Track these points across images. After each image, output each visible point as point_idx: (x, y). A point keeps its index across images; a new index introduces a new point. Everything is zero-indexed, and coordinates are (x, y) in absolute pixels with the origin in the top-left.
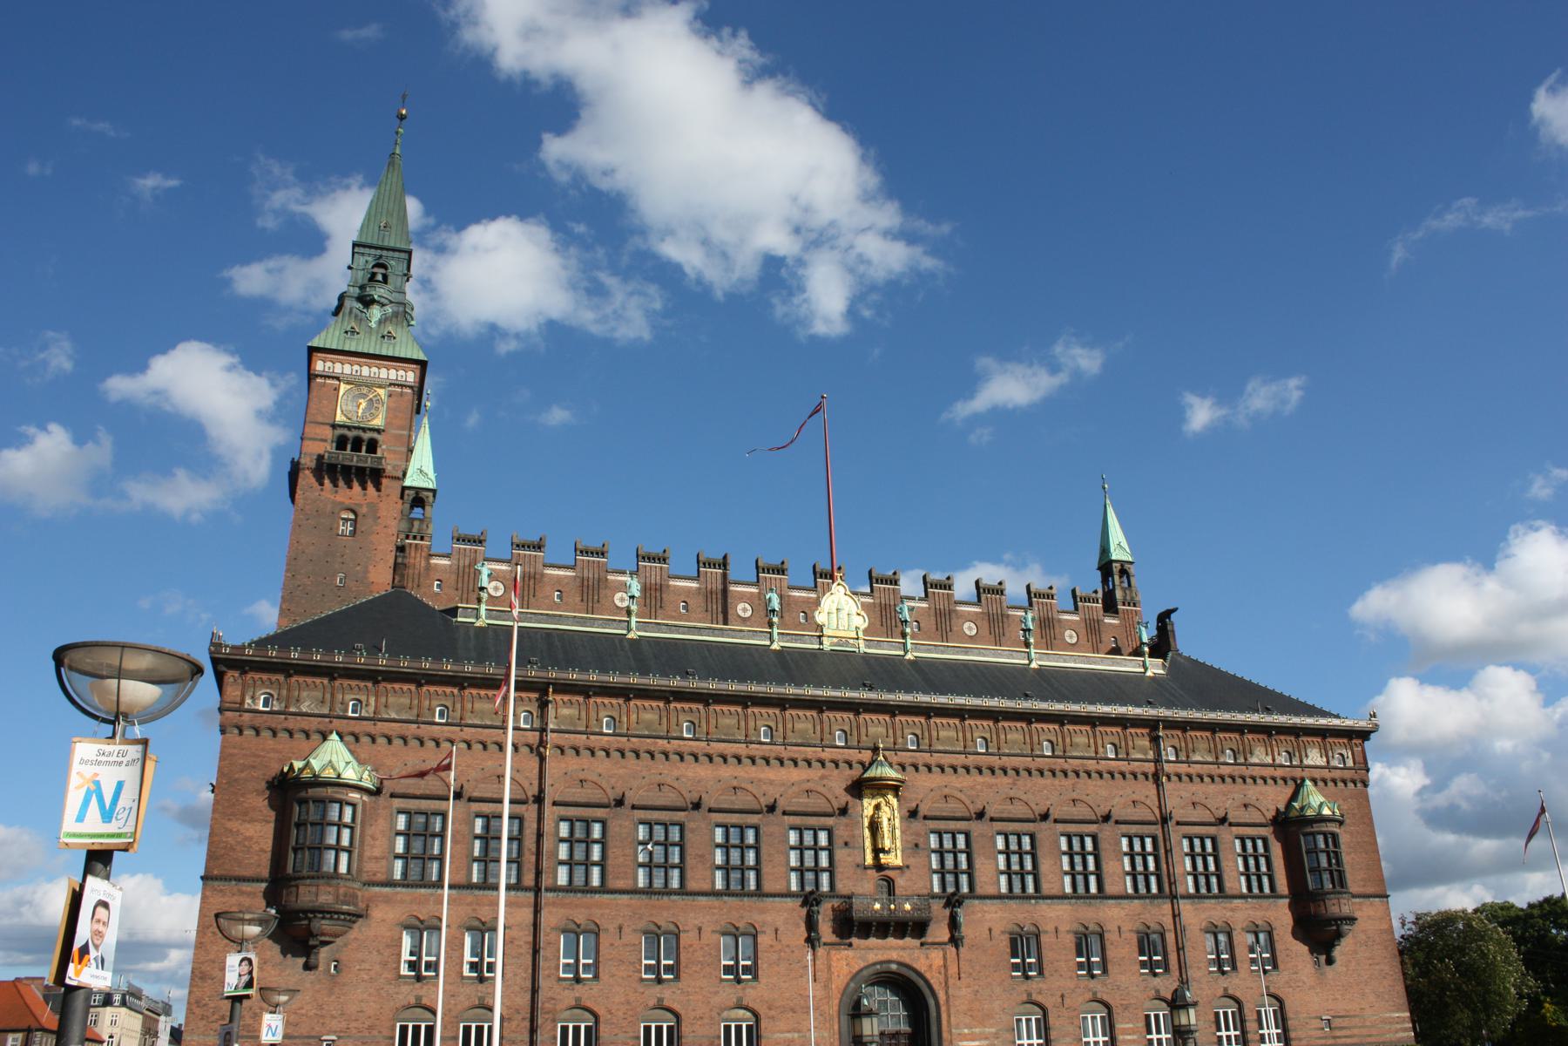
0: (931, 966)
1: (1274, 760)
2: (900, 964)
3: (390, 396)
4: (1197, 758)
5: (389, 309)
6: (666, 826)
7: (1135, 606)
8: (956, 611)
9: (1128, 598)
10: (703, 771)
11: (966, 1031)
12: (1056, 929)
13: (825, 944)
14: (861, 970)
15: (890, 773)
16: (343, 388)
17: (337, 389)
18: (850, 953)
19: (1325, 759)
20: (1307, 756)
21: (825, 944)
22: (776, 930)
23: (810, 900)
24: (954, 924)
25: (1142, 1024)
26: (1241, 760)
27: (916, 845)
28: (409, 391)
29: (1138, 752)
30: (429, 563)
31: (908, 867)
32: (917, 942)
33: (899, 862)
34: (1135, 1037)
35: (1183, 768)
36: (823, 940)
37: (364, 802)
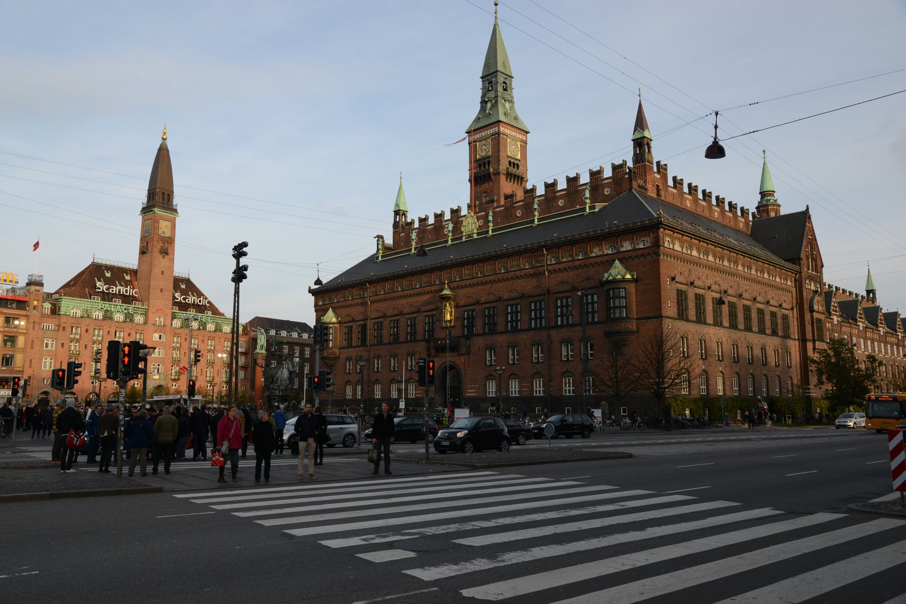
0: (461, 362)
1: (603, 252)
2: (453, 362)
3: (492, 140)
4: (565, 260)
5: (493, 101)
6: (489, 308)
7: (642, 162)
8: (555, 196)
9: (639, 159)
10: (403, 301)
11: (470, 386)
12: (501, 345)
13: (432, 356)
14: (441, 365)
15: (446, 292)
16: (478, 144)
17: (476, 146)
18: (438, 359)
19: (633, 246)
20: (623, 247)
21: (432, 356)
22: (420, 353)
23: (428, 341)
24: (468, 348)
25: (530, 384)
26: (587, 256)
27: (458, 318)
28: (497, 135)
29: (538, 263)
30: (400, 236)
31: (455, 326)
32: (456, 354)
33: (453, 324)
34: (527, 389)
35: (557, 267)
36: (432, 355)
37: (335, 327)
